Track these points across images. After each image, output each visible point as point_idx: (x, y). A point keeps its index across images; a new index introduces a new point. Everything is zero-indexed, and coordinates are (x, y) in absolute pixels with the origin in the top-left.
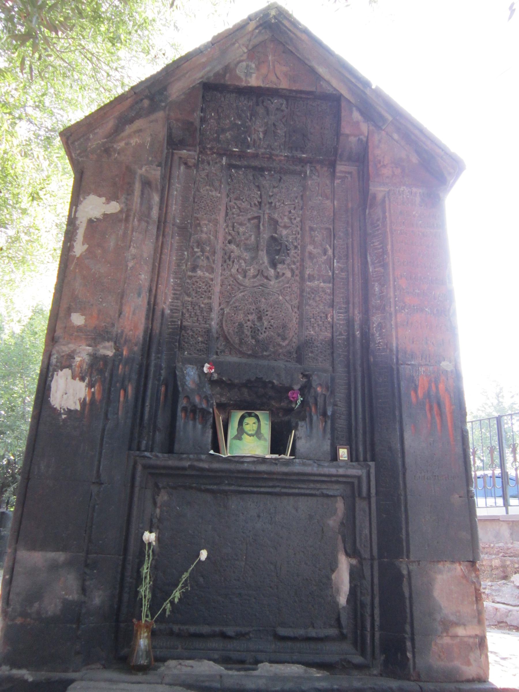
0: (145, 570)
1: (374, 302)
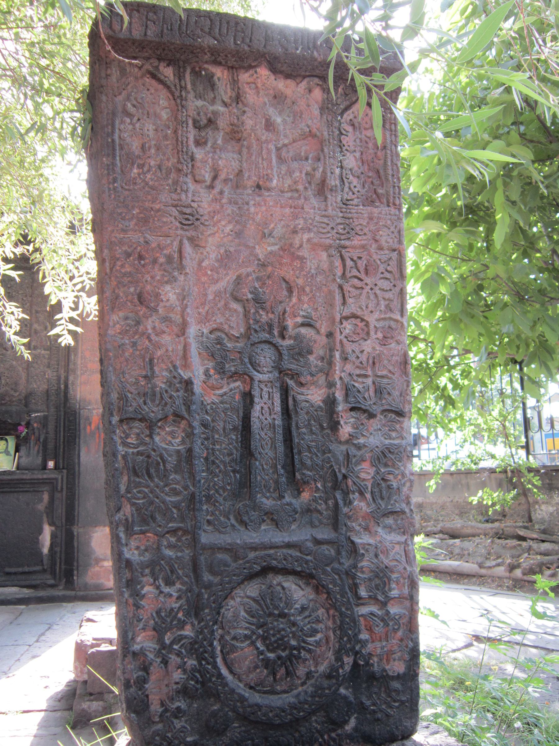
1: (71, 366)
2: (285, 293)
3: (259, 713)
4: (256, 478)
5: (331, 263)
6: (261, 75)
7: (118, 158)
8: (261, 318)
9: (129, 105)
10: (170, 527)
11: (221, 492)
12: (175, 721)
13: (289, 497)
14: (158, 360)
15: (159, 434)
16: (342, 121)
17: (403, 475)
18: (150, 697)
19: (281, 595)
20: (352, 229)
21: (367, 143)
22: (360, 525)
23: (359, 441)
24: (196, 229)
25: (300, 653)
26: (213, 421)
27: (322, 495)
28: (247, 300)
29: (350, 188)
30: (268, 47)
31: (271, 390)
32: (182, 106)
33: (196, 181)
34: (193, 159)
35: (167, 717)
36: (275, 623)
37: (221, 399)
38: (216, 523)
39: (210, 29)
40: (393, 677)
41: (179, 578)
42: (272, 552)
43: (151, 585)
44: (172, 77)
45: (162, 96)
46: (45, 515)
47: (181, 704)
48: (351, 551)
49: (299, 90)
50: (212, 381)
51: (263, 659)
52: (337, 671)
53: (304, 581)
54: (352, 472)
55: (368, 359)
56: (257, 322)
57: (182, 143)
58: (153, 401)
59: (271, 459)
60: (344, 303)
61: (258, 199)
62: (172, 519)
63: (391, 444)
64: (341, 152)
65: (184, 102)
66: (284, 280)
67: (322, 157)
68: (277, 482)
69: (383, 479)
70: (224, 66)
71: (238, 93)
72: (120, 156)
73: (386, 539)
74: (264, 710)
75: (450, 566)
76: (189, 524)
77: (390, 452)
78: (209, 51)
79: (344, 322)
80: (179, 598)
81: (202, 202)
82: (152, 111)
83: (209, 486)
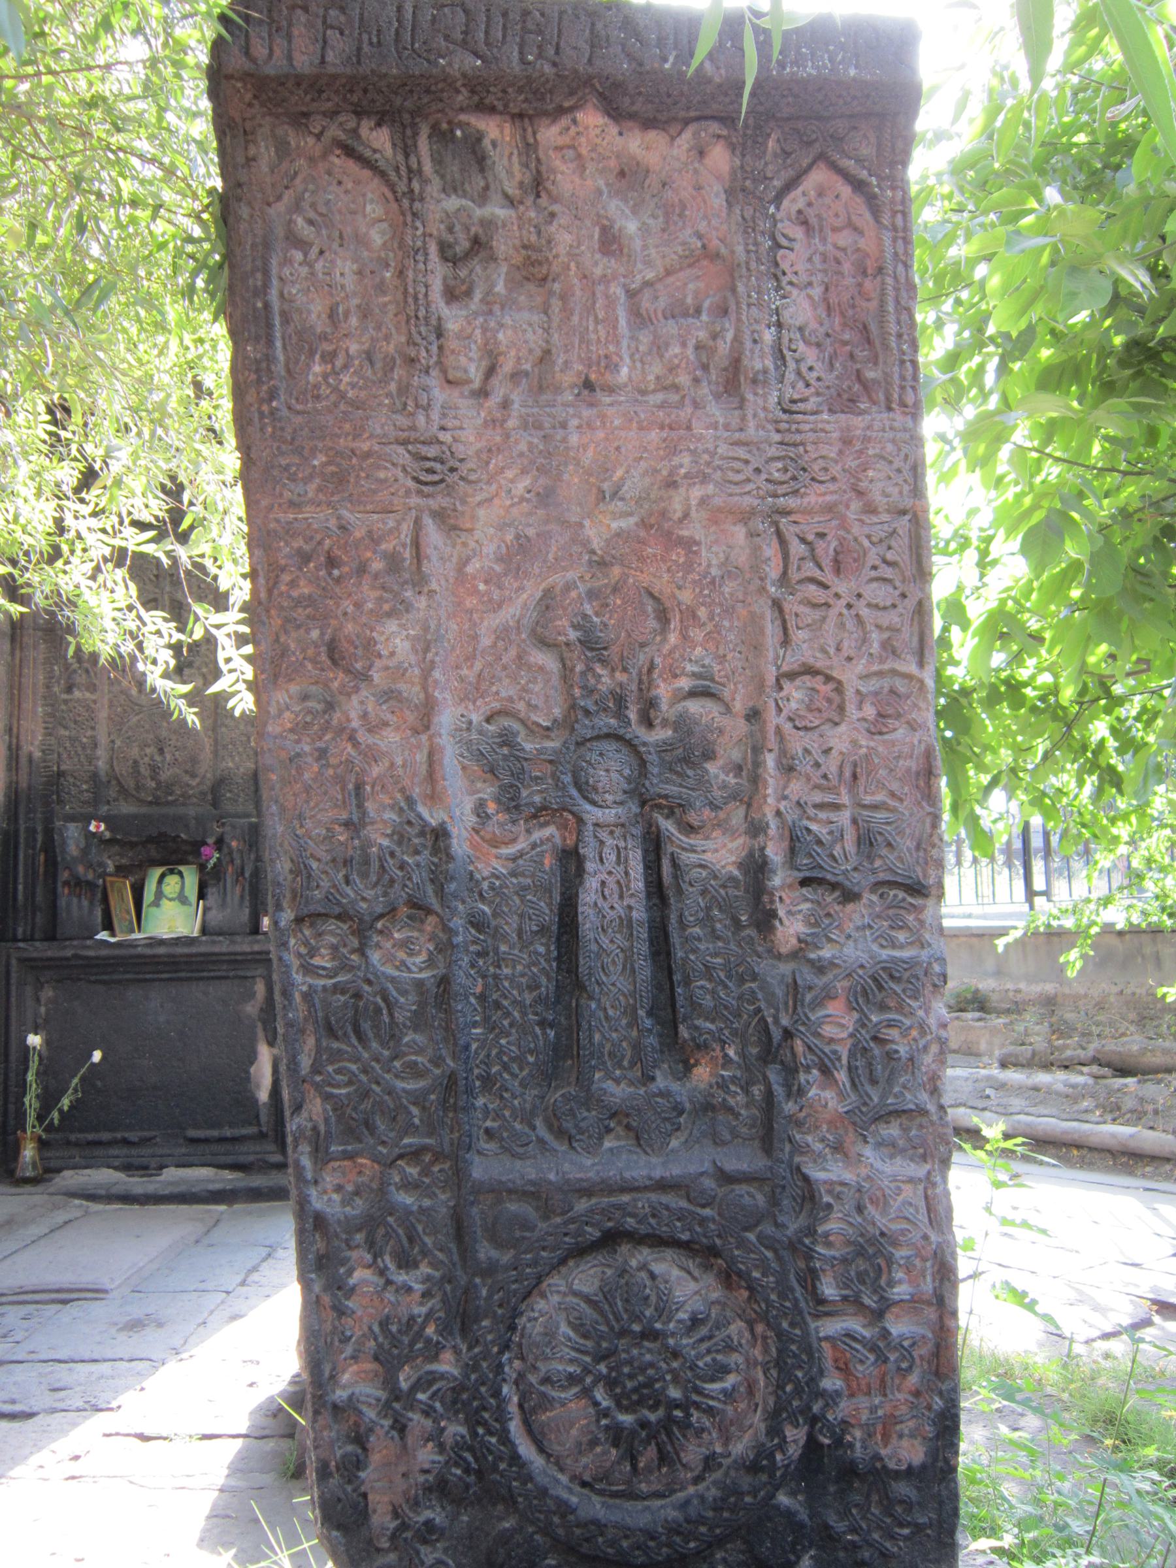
0: (30, 1077)
2: (652, 623)
3: (600, 1539)
4: (591, 1037)
5: (756, 550)
6: (587, 128)
7: (279, 344)
8: (598, 682)
9: (300, 221)
10: (405, 1146)
11: (515, 1068)
12: (423, 1549)
13: (666, 1078)
14: (373, 787)
15: (378, 946)
16: (778, 217)
17: (923, 1028)
18: (370, 1497)
19: (648, 1291)
20: (804, 470)
21: (838, 262)
22: (822, 1140)
23: (821, 953)
24: (450, 490)
25: (688, 1415)
26: (495, 915)
27: (738, 1073)
28: (567, 644)
29: (799, 373)
30: (598, 63)
31: (622, 844)
32: (414, 215)
33: (449, 382)
34: (440, 333)
35: (405, 1540)
36: (635, 1352)
37: (511, 865)
38: (505, 1135)
39: (465, 33)
40: (897, 1472)
41: (425, 1253)
42: (625, 1198)
43: (369, 1267)
44: (389, 151)
45: (370, 195)
46: (259, 1024)
47: (435, 1514)
48: (804, 1198)
49: (675, 152)
50: (492, 828)
51: (607, 1428)
52: (771, 1457)
53: (698, 1260)
54: (804, 1024)
55: (841, 767)
56: (590, 691)
57: (416, 299)
58: (364, 875)
59: (624, 995)
60: (786, 641)
61: (586, 413)
62: (409, 1129)
63: (894, 960)
64: (779, 288)
65: (417, 205)
66: (651, 595)
67: (733, 307)
68: (637, 1046)
69: (875, 1038)
70: (501, 113)
71: (538, 172)
72: (283, 339)
73: (882, 1172)
74: (611, 1533)
75: (1113, 1136)
76: (447, 1140)
77: (892, 977)
78: (464, 85)
79: (787, 685)
80: (426, 1295)
81: (461, 428)
82: (348, 231)
83: (488, 1056)
